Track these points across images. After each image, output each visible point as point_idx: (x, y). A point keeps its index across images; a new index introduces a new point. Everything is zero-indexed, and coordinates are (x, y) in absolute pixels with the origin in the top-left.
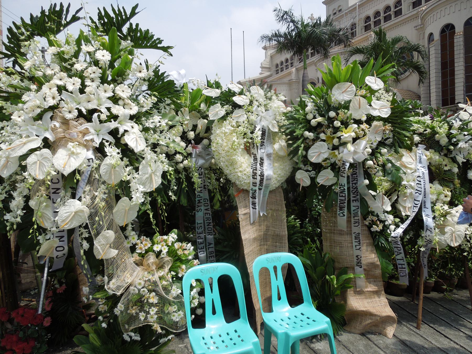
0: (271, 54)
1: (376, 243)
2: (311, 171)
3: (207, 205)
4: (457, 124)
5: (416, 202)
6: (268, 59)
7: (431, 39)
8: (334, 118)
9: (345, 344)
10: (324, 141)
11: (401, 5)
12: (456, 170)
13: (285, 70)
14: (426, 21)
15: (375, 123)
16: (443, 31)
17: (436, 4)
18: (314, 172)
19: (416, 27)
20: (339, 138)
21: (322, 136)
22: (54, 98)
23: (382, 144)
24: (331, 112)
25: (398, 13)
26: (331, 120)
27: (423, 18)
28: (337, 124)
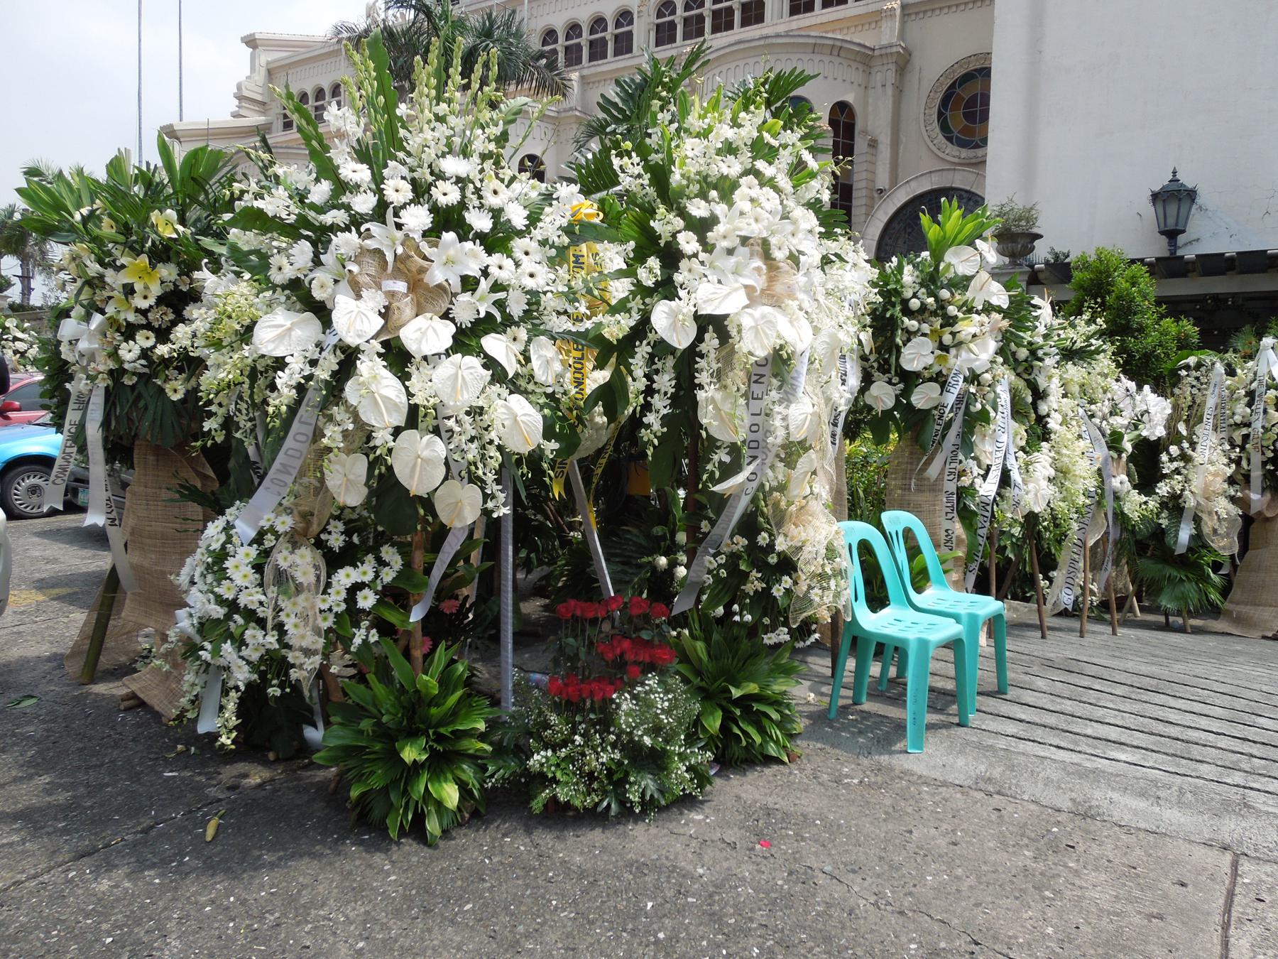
0: (268, 63)
5: (999, 445)
6: (260, 77)
10: (924, 335)
11: (631, 22)
12: (1030, 399)
17: (728, 50)
18: (901, 386)
21: (926, 328)
22: (757, 220)
24: (944, 290)
26: (942, 305)
28: (952, 310)
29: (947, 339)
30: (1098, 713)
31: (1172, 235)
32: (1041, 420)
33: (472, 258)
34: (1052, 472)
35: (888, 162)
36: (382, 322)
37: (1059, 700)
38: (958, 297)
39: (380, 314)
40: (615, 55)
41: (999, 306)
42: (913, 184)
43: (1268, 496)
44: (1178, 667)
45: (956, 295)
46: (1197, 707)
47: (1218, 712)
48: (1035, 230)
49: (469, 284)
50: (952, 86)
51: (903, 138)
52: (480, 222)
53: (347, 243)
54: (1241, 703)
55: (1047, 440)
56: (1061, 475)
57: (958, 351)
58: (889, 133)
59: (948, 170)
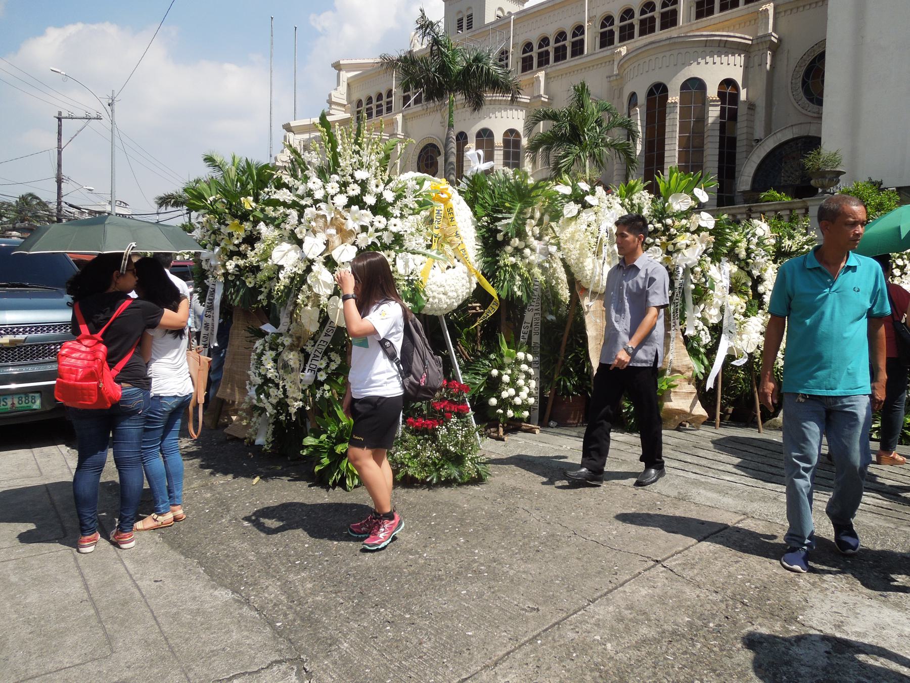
4: (755, 240)
7: (632, 102)
10: (656, 245)
13: (384, 115)
14: (626, 72)
16: (650, 93)
17: (644, 49)
19: (610, 77)
20: (674, 245)
23: (705, 252)
25: (578, 48)
26: (667, 228)
28: (673, 231)
29: (671, 248)
33: (367, 217)
35: (763, 119)
36: (325, 247)
38: (677, 223)
39: (325, 244)
40: (572, 57)
42: (779, 135)
48: (838, 169)
49: (364, 229)
50: (813, 62)
51: (775, 101)
52: (370, 200)
53: (312, 213)
58: (764, 99)
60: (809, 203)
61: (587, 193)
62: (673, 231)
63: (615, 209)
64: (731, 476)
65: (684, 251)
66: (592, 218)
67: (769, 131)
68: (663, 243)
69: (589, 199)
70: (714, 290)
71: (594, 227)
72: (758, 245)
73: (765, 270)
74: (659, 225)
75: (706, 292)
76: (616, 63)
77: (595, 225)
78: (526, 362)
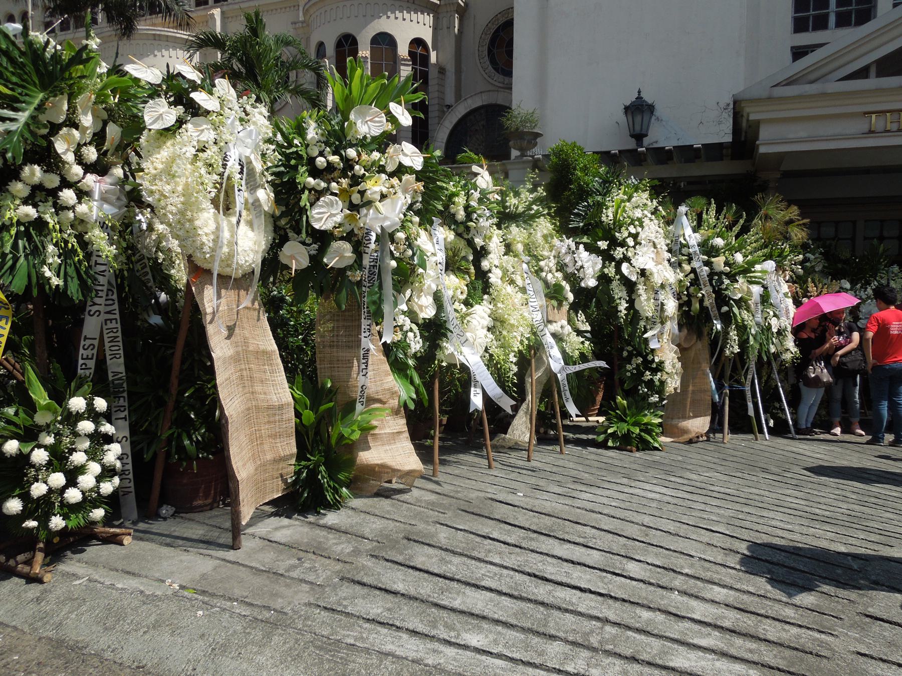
1: (393, 358)
2: (311, 244)
3: (111, 302)
4: (476, 195)
8: (352, 160)
9: (364, 509)
14: (312, 18)
15: (406, 177)
18: (316, 246)
19: (295, 23)
20: (362, 193)
23: (410, 208)
26: (349, 164)
27: (307, 10)
28: (359, 169)
29: (356, 199)
30: (479, 572)
31: (639, 137)
32: (482, 276)
34: (491, 324)
35: (453, 85)
37: (449, 557)
38: (364, 157)
41: (411, 168)
42: (469, 101)
43: (685, 331)
44: (586, 496)
45: (363, 154)
46: (578, 553)
47: (594, 557)
48: (535, 131)
50: (497, 31)
54: (617, 544)
55: (488, 293)
56: (497, 325)
57: (368, 210)
58: (453, 64)
59: (493, 91)
60: (509, 167)
61: (195, 87)
62: (359, 169)
63: (255, 123)
64: (480, 629)
65: (378, 204)
66: (209, 135)
67: (458, 97)
68: (343, 191)
69: (199, 97)
70: (425, 269)
71: (212, 153)
72: (480, 201)
73: (490, 238)
74: (335, 159)
75: (413, 271)
76: (301, 9)
77: (215, 149)
78: (92, 414)
